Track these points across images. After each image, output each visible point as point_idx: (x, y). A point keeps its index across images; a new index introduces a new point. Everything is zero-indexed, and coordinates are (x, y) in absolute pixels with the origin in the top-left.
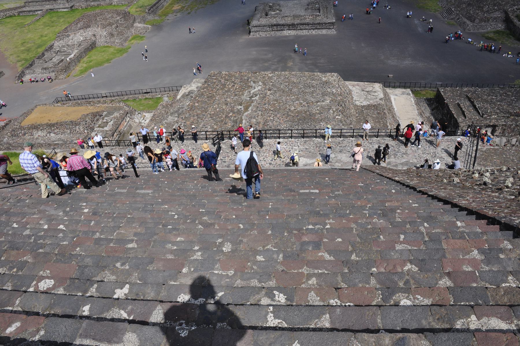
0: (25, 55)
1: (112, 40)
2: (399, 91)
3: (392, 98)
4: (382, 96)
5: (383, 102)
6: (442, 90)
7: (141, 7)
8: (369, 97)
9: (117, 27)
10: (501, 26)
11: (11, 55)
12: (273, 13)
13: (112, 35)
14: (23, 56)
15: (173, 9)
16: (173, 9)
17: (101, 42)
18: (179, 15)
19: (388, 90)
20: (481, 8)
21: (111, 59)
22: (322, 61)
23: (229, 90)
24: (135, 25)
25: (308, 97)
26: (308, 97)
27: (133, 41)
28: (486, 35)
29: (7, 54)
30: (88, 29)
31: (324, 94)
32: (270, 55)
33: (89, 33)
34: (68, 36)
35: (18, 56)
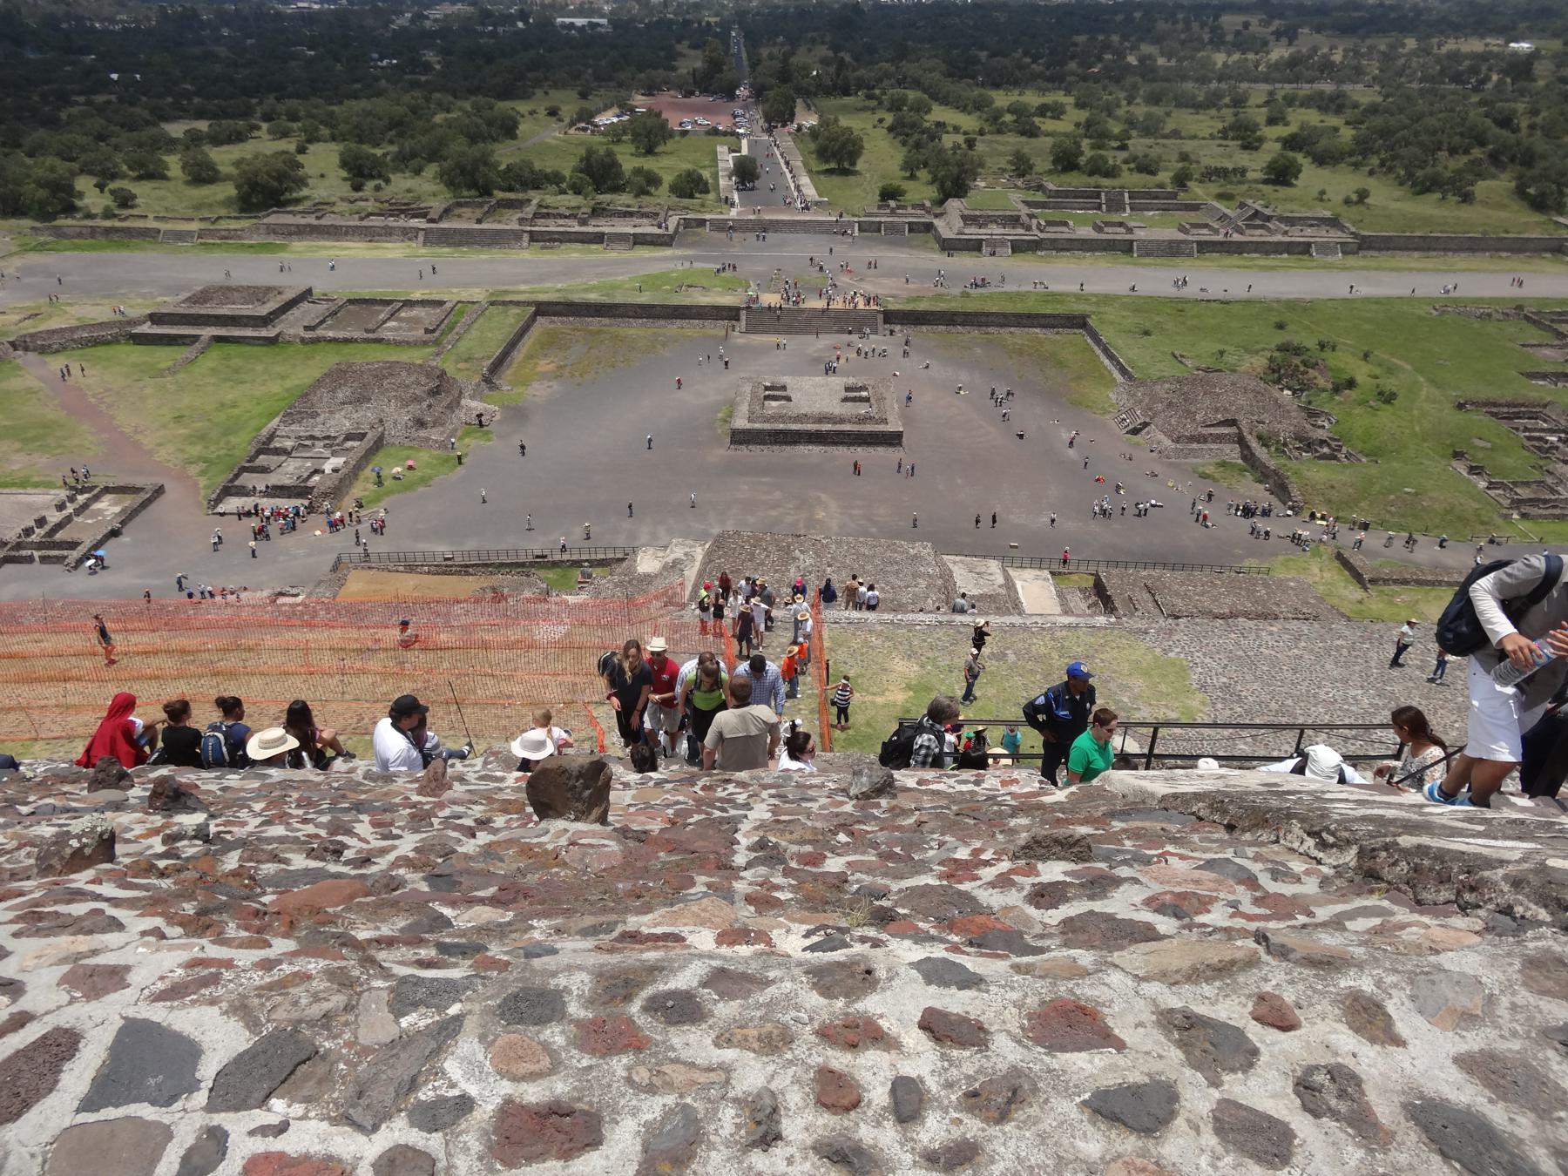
0: (198, 448)
1: (423, 433)
2: (1029, 574)
3: (1019, 585)
4: (1001, 580)
5: (1003, 591)
6: (1102, 575)
7: (466, 361)
8: (981, 582)
9: (430, 406)
10: (1232, 453)
11: (160, 445)
12: (774, 404)
13: (421, 424)
14: (196, 450)
15: (539, 369)
16: (539, 369)
17: (394, 433)
18: (556, 385)
19: (1011, 572)
20: (1190, 415)
21: (430, 478)
22: (882, 511)
23: (762, 564)
24: (463, 402)
25: (892, 579)
26: (892, 579)
27: (467, 441)
28: (1201, 469)
29: (147, 441)
30: (365, 405)
31: (916, 575)
32: (777, 495)
33: (365, 416)
34: (315, 415)
35: (182, 451)
